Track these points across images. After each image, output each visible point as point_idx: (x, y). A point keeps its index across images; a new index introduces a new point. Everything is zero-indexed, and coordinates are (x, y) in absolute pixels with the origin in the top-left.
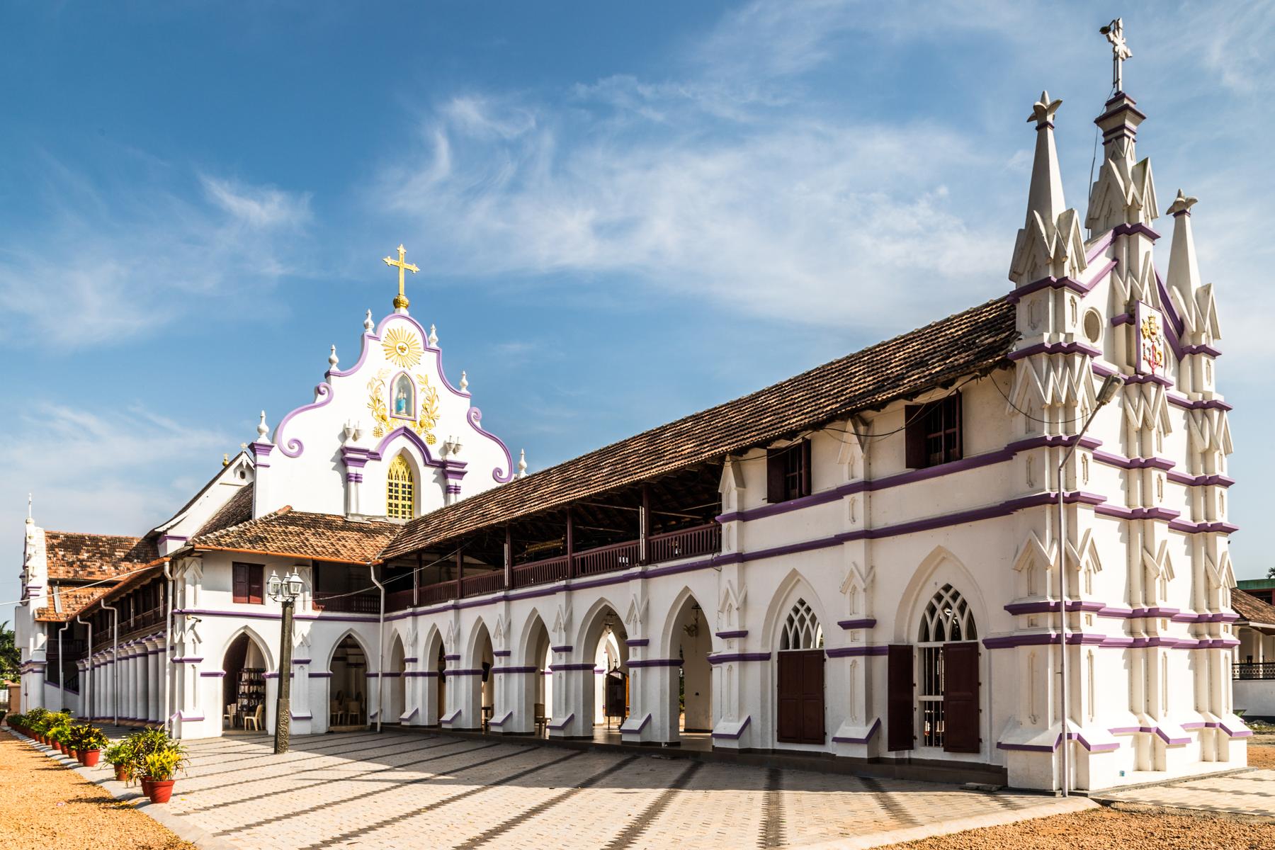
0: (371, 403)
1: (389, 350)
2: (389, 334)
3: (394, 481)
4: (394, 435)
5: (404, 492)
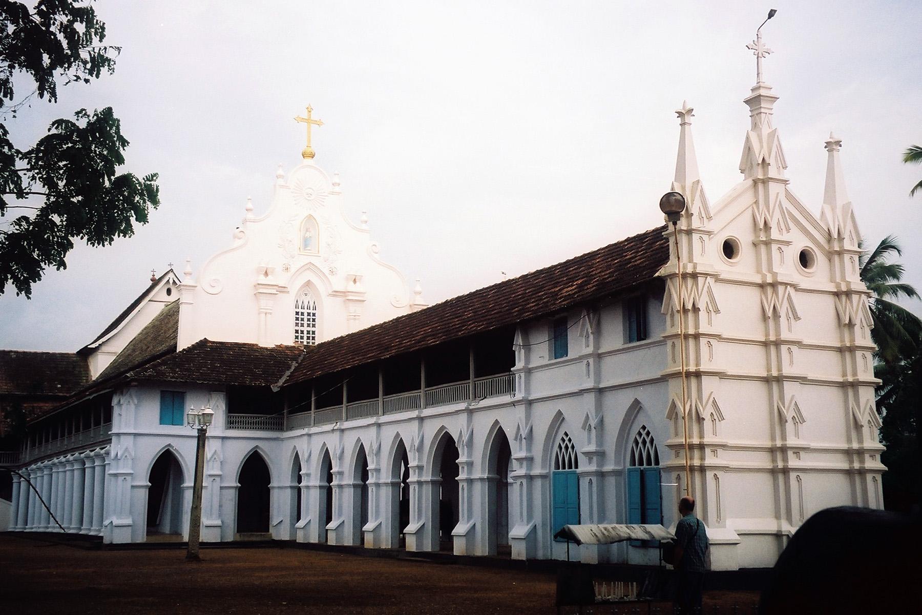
3: (300, 310)
5: (309, 320)
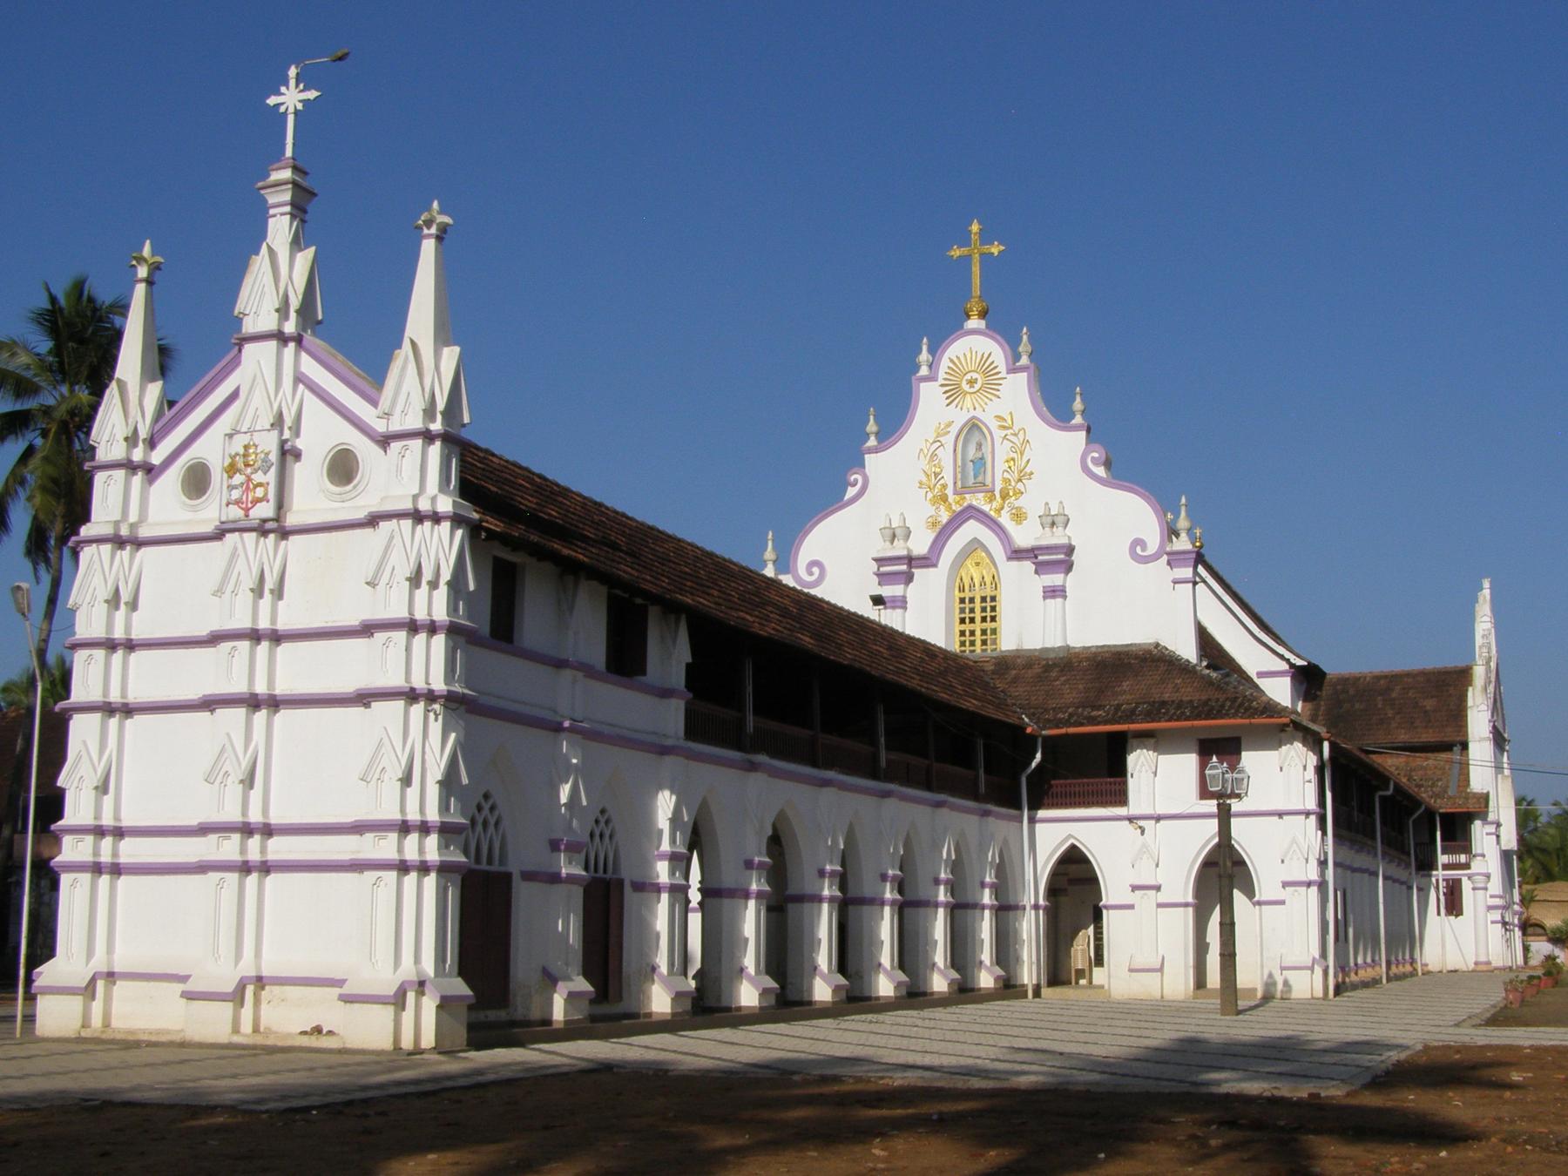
0: (924, 479)
1: (953, 393)
2: (951, 365)
3: (967, 595)
4: (957, 520)
5: (984, 610)
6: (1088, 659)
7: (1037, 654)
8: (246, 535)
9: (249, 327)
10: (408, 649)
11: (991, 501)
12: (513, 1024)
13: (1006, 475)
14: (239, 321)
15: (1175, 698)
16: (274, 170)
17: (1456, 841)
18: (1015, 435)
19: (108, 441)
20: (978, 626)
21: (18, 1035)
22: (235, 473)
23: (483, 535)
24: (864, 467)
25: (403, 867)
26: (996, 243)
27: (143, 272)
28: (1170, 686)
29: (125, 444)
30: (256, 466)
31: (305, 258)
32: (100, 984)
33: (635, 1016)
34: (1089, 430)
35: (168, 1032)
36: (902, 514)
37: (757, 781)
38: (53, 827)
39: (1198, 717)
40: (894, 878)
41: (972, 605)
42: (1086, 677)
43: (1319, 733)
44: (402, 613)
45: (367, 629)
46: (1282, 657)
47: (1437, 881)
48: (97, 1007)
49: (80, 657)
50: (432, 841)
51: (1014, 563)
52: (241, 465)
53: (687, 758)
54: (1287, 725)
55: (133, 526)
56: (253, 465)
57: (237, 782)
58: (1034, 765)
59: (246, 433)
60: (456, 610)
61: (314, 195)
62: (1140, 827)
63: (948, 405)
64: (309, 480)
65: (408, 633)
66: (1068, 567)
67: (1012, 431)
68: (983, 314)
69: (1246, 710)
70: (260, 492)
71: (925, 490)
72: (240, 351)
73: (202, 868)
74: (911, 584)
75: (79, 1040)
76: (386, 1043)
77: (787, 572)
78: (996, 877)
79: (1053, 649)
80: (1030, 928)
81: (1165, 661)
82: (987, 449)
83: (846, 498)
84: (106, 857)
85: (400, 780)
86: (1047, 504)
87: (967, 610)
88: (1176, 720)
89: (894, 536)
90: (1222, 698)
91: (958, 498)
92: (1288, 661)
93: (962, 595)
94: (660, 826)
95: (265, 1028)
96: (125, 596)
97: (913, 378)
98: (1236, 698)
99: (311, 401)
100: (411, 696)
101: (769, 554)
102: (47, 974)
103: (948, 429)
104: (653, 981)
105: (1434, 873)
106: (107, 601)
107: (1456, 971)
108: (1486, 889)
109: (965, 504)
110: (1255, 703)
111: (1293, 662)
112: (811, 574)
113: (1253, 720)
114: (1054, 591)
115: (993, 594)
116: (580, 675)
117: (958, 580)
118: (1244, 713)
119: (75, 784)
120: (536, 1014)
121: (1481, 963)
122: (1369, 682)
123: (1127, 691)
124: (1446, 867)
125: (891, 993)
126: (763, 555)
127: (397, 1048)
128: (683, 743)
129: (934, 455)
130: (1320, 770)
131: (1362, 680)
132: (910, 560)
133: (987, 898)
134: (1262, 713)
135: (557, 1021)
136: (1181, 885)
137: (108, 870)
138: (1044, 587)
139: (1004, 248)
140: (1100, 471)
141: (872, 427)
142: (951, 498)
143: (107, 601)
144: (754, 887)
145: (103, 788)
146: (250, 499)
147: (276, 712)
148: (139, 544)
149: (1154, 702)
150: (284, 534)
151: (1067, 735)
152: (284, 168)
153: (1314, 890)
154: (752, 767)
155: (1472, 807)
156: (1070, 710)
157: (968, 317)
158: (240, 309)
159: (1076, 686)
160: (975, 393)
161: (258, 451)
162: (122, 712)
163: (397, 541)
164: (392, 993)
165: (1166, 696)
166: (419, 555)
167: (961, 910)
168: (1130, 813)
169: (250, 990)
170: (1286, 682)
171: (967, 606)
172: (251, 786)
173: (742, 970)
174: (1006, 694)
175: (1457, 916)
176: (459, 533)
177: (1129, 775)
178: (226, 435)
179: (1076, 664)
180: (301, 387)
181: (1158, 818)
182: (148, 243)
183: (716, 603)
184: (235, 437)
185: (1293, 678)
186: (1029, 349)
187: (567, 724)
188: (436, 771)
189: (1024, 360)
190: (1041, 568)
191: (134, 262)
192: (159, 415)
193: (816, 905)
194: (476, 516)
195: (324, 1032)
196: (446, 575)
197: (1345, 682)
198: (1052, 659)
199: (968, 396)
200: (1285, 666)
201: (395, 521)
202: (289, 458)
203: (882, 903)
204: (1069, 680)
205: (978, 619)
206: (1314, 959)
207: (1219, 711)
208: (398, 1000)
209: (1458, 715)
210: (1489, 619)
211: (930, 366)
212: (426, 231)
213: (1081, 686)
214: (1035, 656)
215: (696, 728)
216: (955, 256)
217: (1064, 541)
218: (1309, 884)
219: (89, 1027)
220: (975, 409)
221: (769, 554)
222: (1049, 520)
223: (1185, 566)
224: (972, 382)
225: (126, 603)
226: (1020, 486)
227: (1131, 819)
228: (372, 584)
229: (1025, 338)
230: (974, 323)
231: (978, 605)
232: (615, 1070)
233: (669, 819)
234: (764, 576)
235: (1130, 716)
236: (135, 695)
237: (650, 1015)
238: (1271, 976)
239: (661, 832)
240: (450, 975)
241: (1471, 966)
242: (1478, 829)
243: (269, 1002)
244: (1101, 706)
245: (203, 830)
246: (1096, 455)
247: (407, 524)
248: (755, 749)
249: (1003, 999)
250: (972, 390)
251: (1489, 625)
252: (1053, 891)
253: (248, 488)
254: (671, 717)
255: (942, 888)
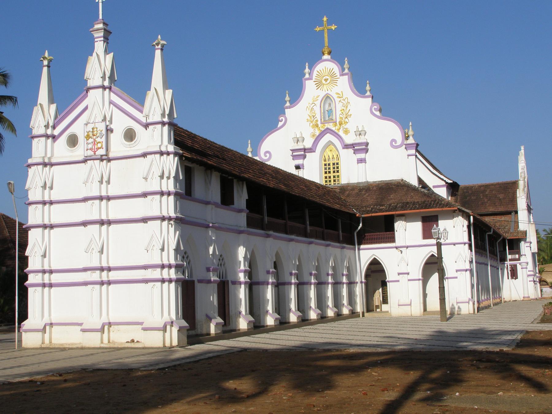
0: (309, 118)
1: (319, 84)
2: (318, 74)
3: (327, 163)
5: (334, 168)
6: (376, 186)
7: (355, 185)
8: (95, 161)
9: (90, 84)
10: (161, 202)
11: (335, 126)
12: (197, 335)
13: (341, 116)
14: (86, 81)
15: (412, 201)
16: (95, 24)
17: (513, 249)
18: (344, 100)
19: (38, 127)
20: (332, 175)
21: (16, 348)
22: (89, 138)
23: (184, 159)
24: (285, 114)
25: (163, 281)
26: (333, 25)
27: (46, 63)
28: (409, 196)
29: (45, 128)
30: (97, 135)
31: (110, 57)
32: (48, 328)
33: (235, 330)
34: (372, 98)
35: (76, 344)
36: (301, 132)
37: (270, 241)
38: (25, 271)
39: (422, 208)
40: (315, 274)
41: (329, 167)
42: (376, 193)
43: (469, 213)
44: (158, 189)
45: (145, 195)
46: (442, 180)
47: (507, 265)
48: (47, 336)
49: (31, 208)
50: (173, 270)
51: (346, 150)
52: (91, 134)
53: (248, 234)
54: (456, 210)
55: (49, 158)
56: (96, 135)
57: (97, 252)
58: (359, 228)
59: (92, 123)
60: (176, 186)
61: (111, 33)
62: (401, 251)
63: (317, 89)
64: (117, 139)
65: (160, 195)
66: (366, 151)
67: (342, 99)
68: (329, 53)
69: (440, 205)
70: (99, 145)
71: (309, 123)
72: (87, 92)
73: (85, 284)
74: (305, 159)
75: (41, 348)
76: (161, 345)
77: (257, 156)
78: (348, 271)
79: (362, 183)
80: (359, 290)
81: (406, 186)
82: (333, 106)
83: (279, 126)
84: (47, 281)
85: (161, 249)
86: (357, 127)
87: (327, 169)
88: (413, 210)
89: (298, 140)
90: (430, 200)
91: (322, 125)
92: (445, 181)
93: (325, 163)
94: (240, 260)
95: (112, 341)
96: (48, 185)
97: (303, 79)
98: (436, 200)
99: (115, 110)
100: (163, 219)
101: (249, 149)
102: (26, 324)
103: (318, 99)
104: (240, 317)
105: (506, 262)
106: (42, 187)
107: (516, 301)
108: (527, 268)
109: (325, 128)
110: (443, 202)
111: (447, 181)
112: (266, 156)
113: (443, 209)
114: (361, 160)
115: (337, 162)
116: (214, 206)
117: (324, 157)
118: (439, 206)
119: (33, 255)
120: (204, 332)
121: (526, 297)
122: (477, 188)
123: (393, 199)
124: (510, 260)
125: (316, 318)
126: (247, 149)
127: (164, 346)
128: (246, 229)
129: (312, 109)
130: (469, 227)
131: (474, 187)
132: (305, 150)
133: (345, 280)
134: (447, 206)
135: (212, 334)
136: (417, 272)
137: (48, 286)
138: (357, 159)
139: (337, 27)
140: (378, 113)
141: (287, 98)
142: (320, 125)
143: (42, 187)
144: (270, 281)
145: (44, 256)
146: (96, 148)
147: (109, 226)
148: (52, 165)
149: (404, 203)
150: (109, 160)
151: (372, 217)
152: (100, 23)
153: (468, 272)
154: (268, 236)
155: (520, 236)
156: (372, 207)
157: (324, 54)
158: (87, 77)
159: (373, 197)
160: (327, 84)
161: (98, 130)
162: (50, 227)
163: (154, 162)
164: (162, 326)
165: (408, 200)
166: (163, 167)
167: (337, 284)
168: (396, 245)
169: (106, 327)
170: (445, 189)
171: (327, 167)
172: (102, 253)
173: (267, 312)
174: (346, 201)
175: (515, 279)
176: (176, 158)
177: (395, 231)
178: (85, 124)
179: (372, 188)
180: (111, 105)
181: (407, 247)
182: (47, 51)
183: (253, 176)
184: (88, 125)
185: (447, 188)
186: (348, 66)
187: (211, 225)
188: (173, 245)
189: (346, 71)
190: (356, 152)
191: (42, 59)
192: (56, 117)
193: (289, 286)
194: (181, 152)
195: (135, 341)
196: (173, 174)
197: (467, 188)
198: (362, 186)
199: (325, 85)
200: (444, 183)
201: (153, 155)
202: (109, 132)
203: (311, 284)
204: (369, 195)
205: (332, 172)
206: (469, 299)
207: (430, 206)
208: (164, 329)
209: (513, 200)
210: (524, 162)
211: (309, 74)
212: (157, 47)
213: (374, 197)
214: (355, 186)
215: (251, 223)
216: (317, 31)
217: (365, 141)
218: (466, 270)
219: (44, 343)
220: (328, 90)
221: (249, 149)
222: (359, 133)
223: (412, 149)
224: (326, 80)
225: (49, 187)
226: (346, 120)
227: (397, 248)
228: (146, 179)
229: (346, 62)
230: (326, 57)
231: (331, 166)
232: (248, 350)
233: (243, 257)
234: (248, 157)
235: (395, 209)
236: (54, 221)
237: (239, 330)
238: (453, 305)
239: (240, 262)
240: (180, 319)
241: (522, 299)
242: (522, 244)
243: (113, 331)
244: (383, 205)
245: (85, 270)
246: (376, 107)
247: (158, 156)
248: (269, 229)
249: (352, 318)
250: (326, 83)
251: (524, 164)
252: (367, 276)
253: (95, 143)
254: (242, 219)
255: (330, 277)
